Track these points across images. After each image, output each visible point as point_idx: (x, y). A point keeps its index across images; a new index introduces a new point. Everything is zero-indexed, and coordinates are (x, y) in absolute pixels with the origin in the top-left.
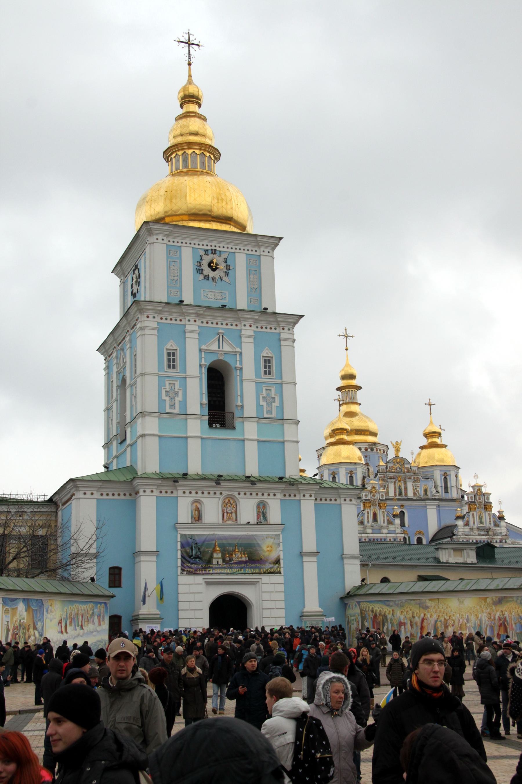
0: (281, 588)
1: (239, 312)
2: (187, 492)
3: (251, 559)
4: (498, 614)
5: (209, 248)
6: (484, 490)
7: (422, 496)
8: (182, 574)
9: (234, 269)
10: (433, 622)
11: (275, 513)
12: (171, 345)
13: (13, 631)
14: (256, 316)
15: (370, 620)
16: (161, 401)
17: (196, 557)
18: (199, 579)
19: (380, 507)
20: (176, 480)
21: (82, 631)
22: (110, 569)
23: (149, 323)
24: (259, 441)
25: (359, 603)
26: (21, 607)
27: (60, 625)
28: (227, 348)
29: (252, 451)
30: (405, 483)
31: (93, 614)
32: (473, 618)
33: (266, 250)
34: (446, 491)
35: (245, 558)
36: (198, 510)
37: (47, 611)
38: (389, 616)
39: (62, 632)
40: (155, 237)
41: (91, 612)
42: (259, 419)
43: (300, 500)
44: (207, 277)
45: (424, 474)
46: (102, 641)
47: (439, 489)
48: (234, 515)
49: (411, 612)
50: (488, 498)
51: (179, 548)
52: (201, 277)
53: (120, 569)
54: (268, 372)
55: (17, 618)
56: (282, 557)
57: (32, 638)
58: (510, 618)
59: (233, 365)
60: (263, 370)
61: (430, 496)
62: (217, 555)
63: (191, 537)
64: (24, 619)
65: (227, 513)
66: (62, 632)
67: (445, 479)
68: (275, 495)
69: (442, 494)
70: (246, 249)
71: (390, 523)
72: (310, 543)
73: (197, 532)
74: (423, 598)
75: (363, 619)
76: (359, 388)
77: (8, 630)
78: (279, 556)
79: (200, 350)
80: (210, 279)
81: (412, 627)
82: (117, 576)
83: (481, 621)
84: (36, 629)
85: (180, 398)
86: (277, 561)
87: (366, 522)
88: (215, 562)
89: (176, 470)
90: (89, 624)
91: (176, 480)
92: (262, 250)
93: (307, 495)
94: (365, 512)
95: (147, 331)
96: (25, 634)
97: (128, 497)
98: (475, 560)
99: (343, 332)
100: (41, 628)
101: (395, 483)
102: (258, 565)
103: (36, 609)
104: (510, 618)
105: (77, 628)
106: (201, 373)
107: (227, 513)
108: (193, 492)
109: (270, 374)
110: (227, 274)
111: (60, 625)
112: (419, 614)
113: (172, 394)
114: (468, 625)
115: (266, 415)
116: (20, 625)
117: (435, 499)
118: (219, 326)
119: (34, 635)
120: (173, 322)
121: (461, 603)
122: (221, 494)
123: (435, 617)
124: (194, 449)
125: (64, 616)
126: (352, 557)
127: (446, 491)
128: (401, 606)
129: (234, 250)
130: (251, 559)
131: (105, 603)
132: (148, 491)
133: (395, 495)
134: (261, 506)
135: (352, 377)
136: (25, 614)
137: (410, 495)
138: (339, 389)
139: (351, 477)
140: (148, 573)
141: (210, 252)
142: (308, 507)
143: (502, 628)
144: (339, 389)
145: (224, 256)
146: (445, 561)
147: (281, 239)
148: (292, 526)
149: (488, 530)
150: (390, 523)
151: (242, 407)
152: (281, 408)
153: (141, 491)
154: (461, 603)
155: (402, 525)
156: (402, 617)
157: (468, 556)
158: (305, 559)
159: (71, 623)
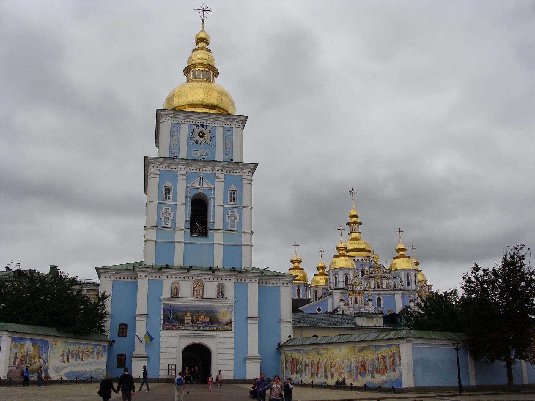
0: (232, 340)
1: (214, 163)
2: (170, 277)
3: (211, 321)
4: (361, 358)
5: (199, 124)
6: (428, 283)
7: (393, 288)
8: (163, 329)
9: (215, 136)
10: (324, 364)
11: (230, 290)
12: (168, 184)
13: (20, 358)
14: (225, 165)
15: (290, 363)
16: (159, 220)
17: (173, 318)
18: (175, 333)
19: (359, 294)
20: (160, 269)
21: (82, 363)
22: (120, 325)
23: (154, 170)
24: (224, 245)
25: (284, 351)
26: (28, 344)
27: (62, 357)
28: (205, 185)
29: (218, 251)
30: (381, 280)
31: (93, 352)
32: (346, 361)
33: (237, 124)
34: (408, 285)
35: (207, 320)
36: (177, 288)
37: (51, 347)
38: (300, 360)
39: (64, 362)
40: (164, 118)
41: (91, 351)
42: (225, 230)
43: (248, 283)
44: (197, 142)
45: (392, 273)
46: (100, 369)
47: (404, 284)
48: (201, 292)
49: (312, 357)
50: (431, 289)
51: (162, 313)
52: (193, 142)
53: (127, 325)
54: (233, 199)
55: (24, 351)
56: (233, 320)
57: (37, 364)
58: (367, 361)
59: (209, 197)
60: (229, 199)
61: (397, 288)
62: (188, 318)
63: (170, 305)
64: (30, 351)
65: (197, 291)
66: (64, 362)
67: (408, 277)
68: (230, 280)
70: (224, 124)
71: (366, 304)
72: (253, 310)
73: (175, 302)
74: (319, 347)
75: (286, 361)
76: (360, 223)
77: (16, 358)
78: (231, 319)
79: (187, 187)
80: (199, 143)
81: (312, 367)
82: (125, 330)
83: (351, 363)
84: (41, 358)
85: (172, 217)
86: (230, 323)
87: (350, 304)
88: (186, 322)
90: (89, 358)
91: (160, 269)
92: (234, 124)
93: (253, 280)
94: (350, 298)
95: (152, 176)
96: (31, 361)
97: (133, 280)
98: (382, 324)
99: (350, 189)
100: (45, 358)
101: (374, 280)
102: (216, 325)
103: (42, 347)
104: (367, 361)
105: (78, 360)
106: (186, 201)
107: (197, 291)
108: (174, 277)
109: (234, 201)
110: (210, 139)
111: (62, 357)
112: (317, 358)
113: (167, 215)
114: (343, 366)
115: (230, 228)
116: (27, 355)
117: (401, 290)
118: (201, 171)
119: (39, 362)
120: (170, 169)
121: (340, 351)
122: (193, 278)
123: (325, 360)
124: (179, 250)
125: (67, 351)
126: (286, 321)
127: (408, 285)
128: (307, 353)
129: (216, 125)
130: (211, 321)
131: (104, 346)
132: (143, 276)
133: (375, 288)
134: (221, 287)
136: (32, 348)
137: (385, 287)
138: (348, 224)
139: (346, 277)
140: (141, 328)
141: (200, 126)
142: (253, 288)
143: (363, 367)
144: (348, 224)
145: (209, 128)
146: (360, 325)
147: (247, 117)
148: (241, 300)
150: (366, 304)
151: (214, 223)
152: (240, 224)
153: (139, 275)
154: (340, 351)
155: (379, 305)
156: (307, 360)
157: (377, 321)
158: (249, 322)
159: (72, 357)
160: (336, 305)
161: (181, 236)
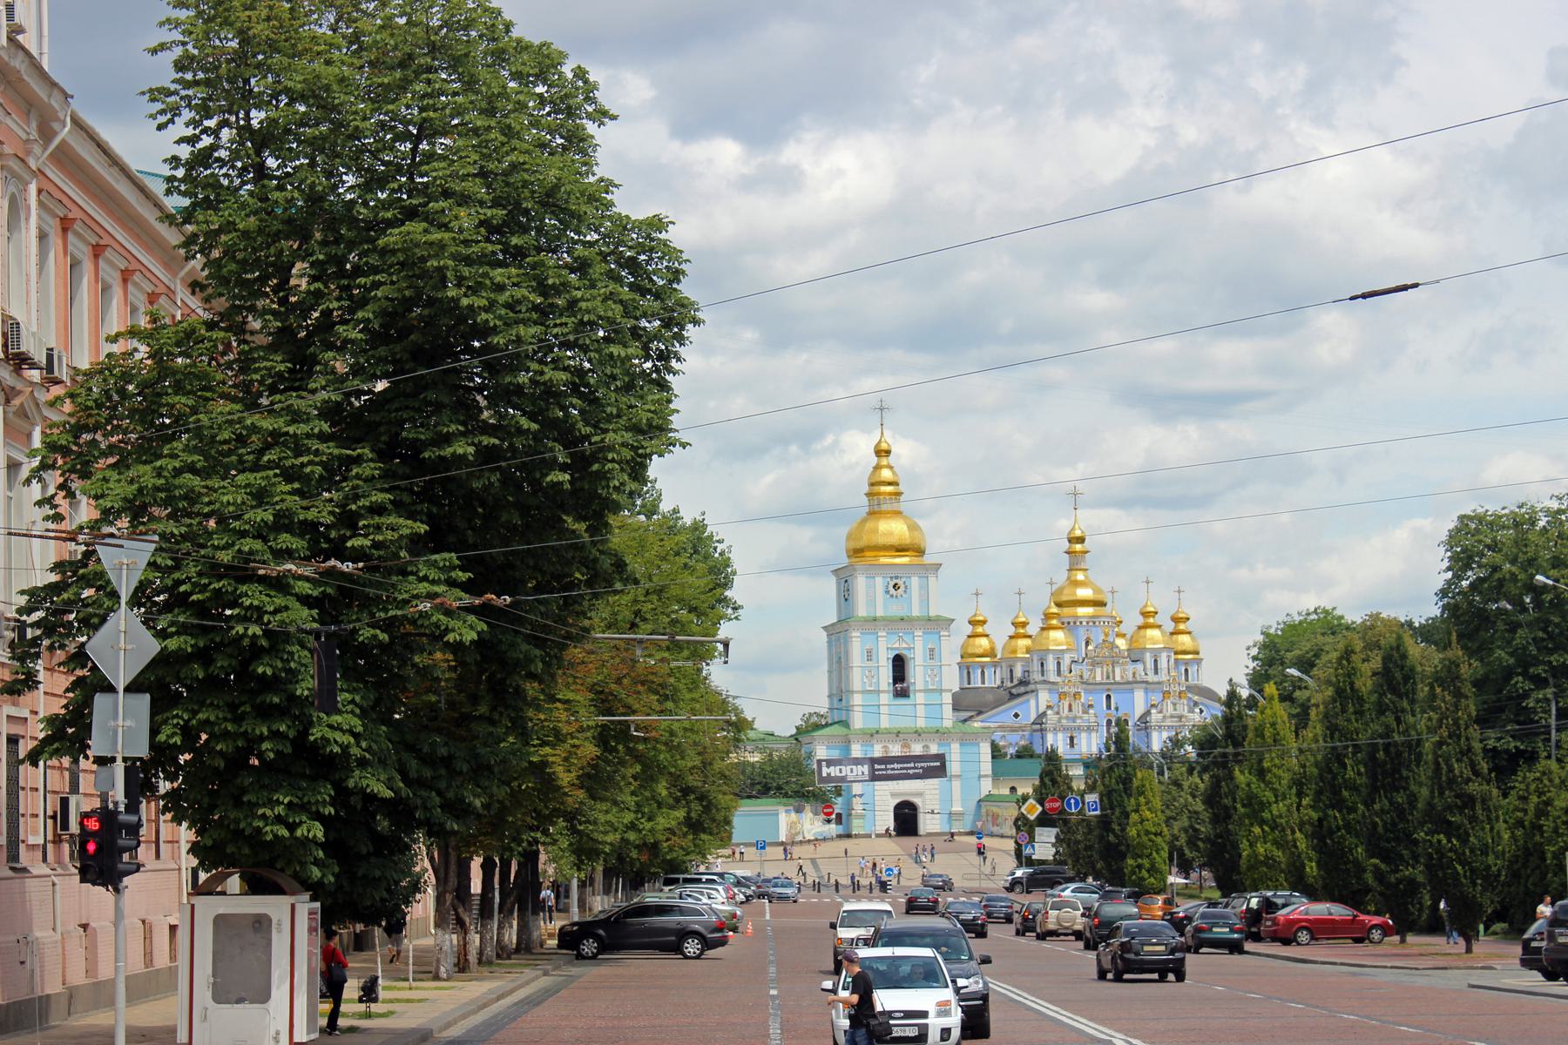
29: (921, 711)
69: (1151, 677)
71: (1085, 712)
89: (872, 725)
135: (1081, 540)
137: (1118, 678)
149: (1180, 717)
150: (1085, 712)
160: (1042, 708)
161: (886, 698)
